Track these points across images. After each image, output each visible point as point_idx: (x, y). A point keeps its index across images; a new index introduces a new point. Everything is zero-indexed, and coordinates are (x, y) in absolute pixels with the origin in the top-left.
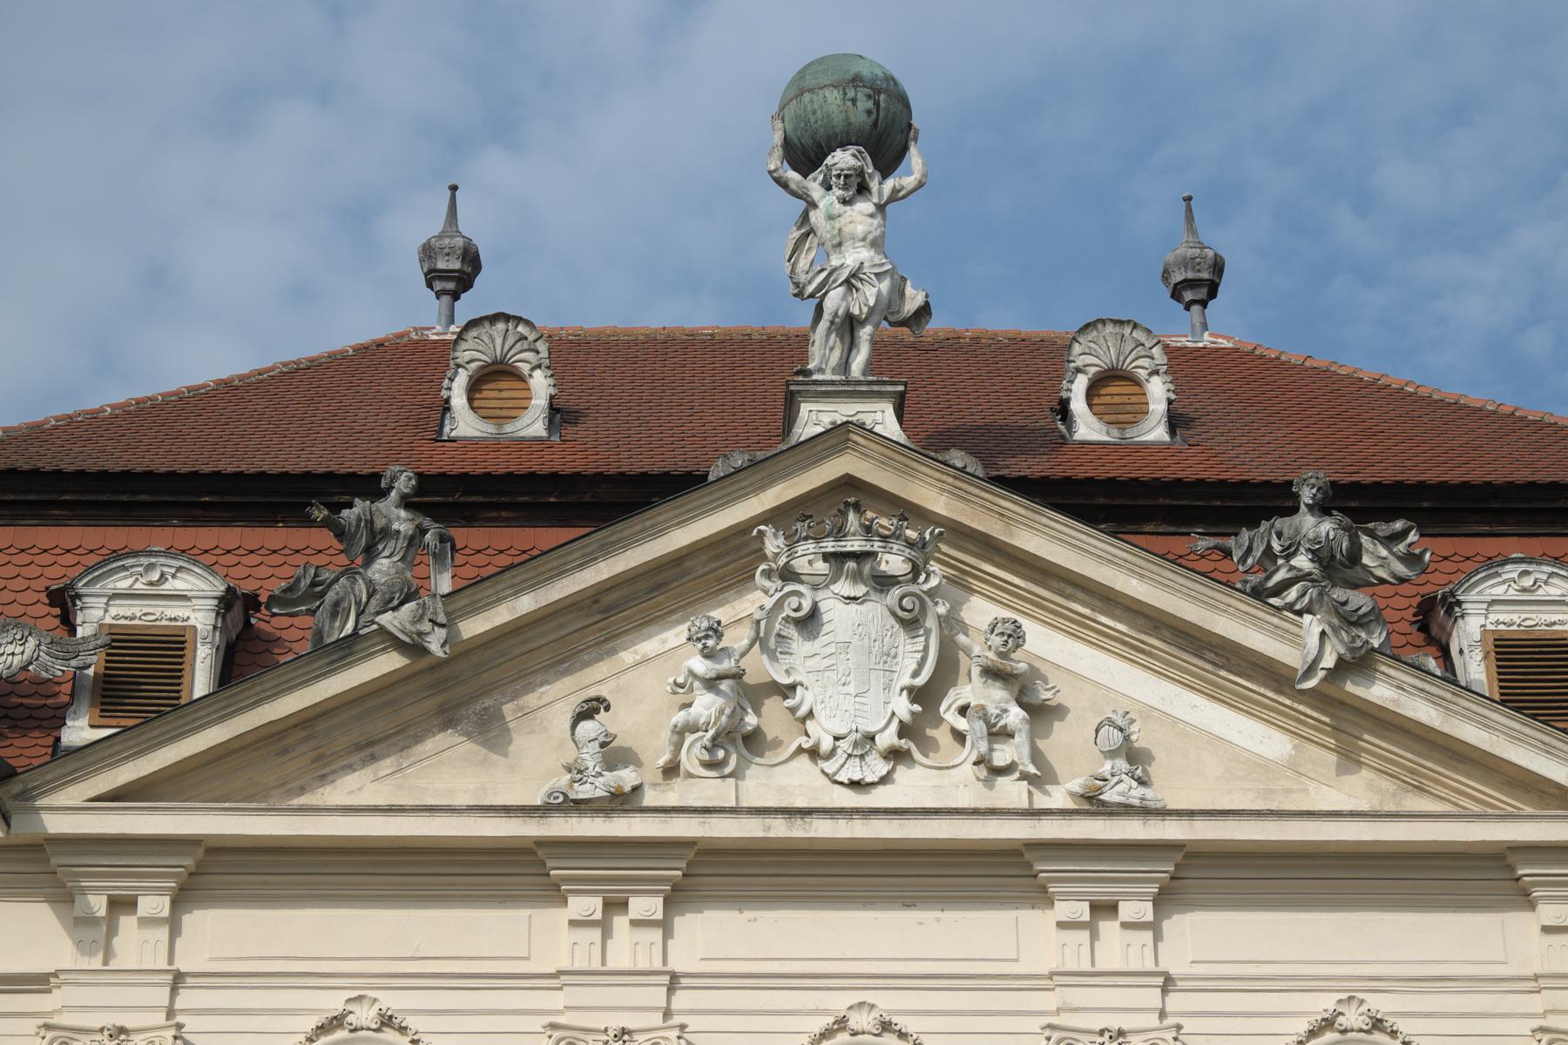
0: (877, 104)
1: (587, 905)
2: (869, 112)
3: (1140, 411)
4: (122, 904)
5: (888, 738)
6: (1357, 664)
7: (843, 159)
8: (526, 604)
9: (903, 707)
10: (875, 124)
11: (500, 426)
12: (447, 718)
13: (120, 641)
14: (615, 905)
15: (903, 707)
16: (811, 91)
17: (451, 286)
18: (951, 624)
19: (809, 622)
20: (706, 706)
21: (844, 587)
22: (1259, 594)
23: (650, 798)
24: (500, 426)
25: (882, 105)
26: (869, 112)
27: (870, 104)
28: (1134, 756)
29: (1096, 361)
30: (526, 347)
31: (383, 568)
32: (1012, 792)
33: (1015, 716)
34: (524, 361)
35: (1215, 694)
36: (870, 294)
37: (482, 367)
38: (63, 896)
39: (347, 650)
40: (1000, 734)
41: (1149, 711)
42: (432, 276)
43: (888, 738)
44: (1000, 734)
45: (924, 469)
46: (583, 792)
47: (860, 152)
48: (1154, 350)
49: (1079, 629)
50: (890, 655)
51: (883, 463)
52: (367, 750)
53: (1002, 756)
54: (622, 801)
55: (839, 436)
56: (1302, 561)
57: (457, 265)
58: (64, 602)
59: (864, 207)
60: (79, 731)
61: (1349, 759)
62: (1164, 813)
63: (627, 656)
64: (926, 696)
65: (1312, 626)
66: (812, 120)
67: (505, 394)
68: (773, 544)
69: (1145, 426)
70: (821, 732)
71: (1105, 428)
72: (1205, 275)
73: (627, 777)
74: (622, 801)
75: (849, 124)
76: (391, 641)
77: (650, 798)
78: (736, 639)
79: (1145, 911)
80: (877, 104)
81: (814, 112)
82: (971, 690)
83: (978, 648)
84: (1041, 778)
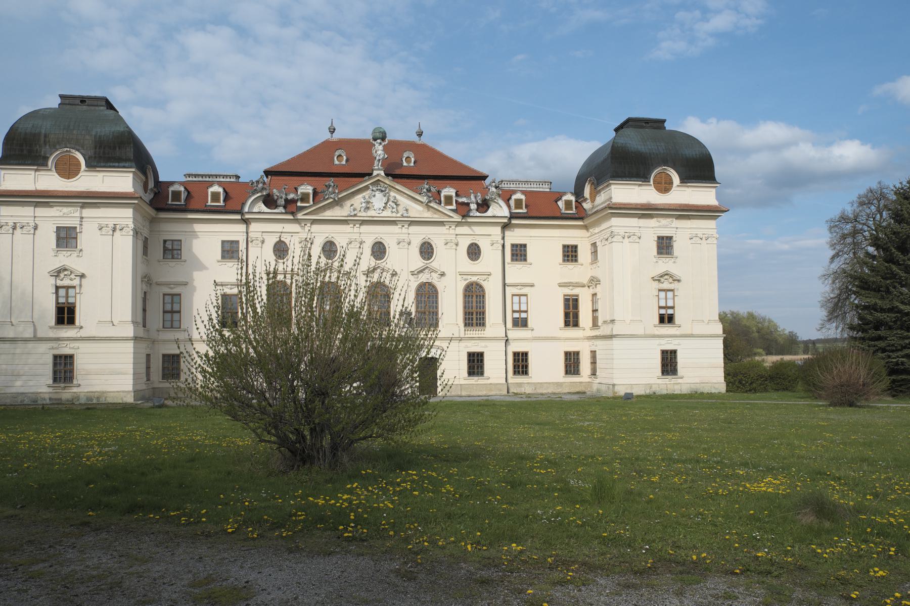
1: (352, 225)
3: (411, 162)
4: (305, 225)
5: (382, 208)
6: (430, 202)
7: (379, 141)
8: (345, 194)
9: (384, 205)
12: (337, 205)
13: (302, 193)
14: (355, 225)
15: (384, 205)
18: (389, 196)
19: (374, 196)
20: (364, 205)
21: (378, 192)
22: (420, 194)
23: (358, 215)
28: (407, 210)
31: (330, 189)
32: (394, 215)
33: (395, 206)
34: (343, 155)
35: (416, 203)
36: (381, 157)
38: (300, 224)
39: (328, 199)
40: (393, 208)
41: (408, 205)
42: (330, 131)
43: (382, 208)
44: (393, 208)
46: (352, 214)
49: (402, 196)
50: (382, 199)
52: (329, 208)
53: (394, 210)
54: (355, 215)
55: (378, 175)
56: (425, 190)
58: (296, 189)
59: (381, 146)
60: (299, 204)
61: (429, 210)
62: (409, 217)
63: (356, 198)
64: (386, 204)
65: (425, 198)
68: (371, 187)
70: (375, 208)
73: (356, 212)
74: (355, 215)
76: (331, 198)
77: (358, 215)
78: (367, 197)
79: (407, 227)
82: (390, 203)
83: (392, 199)
84: (398, 212)
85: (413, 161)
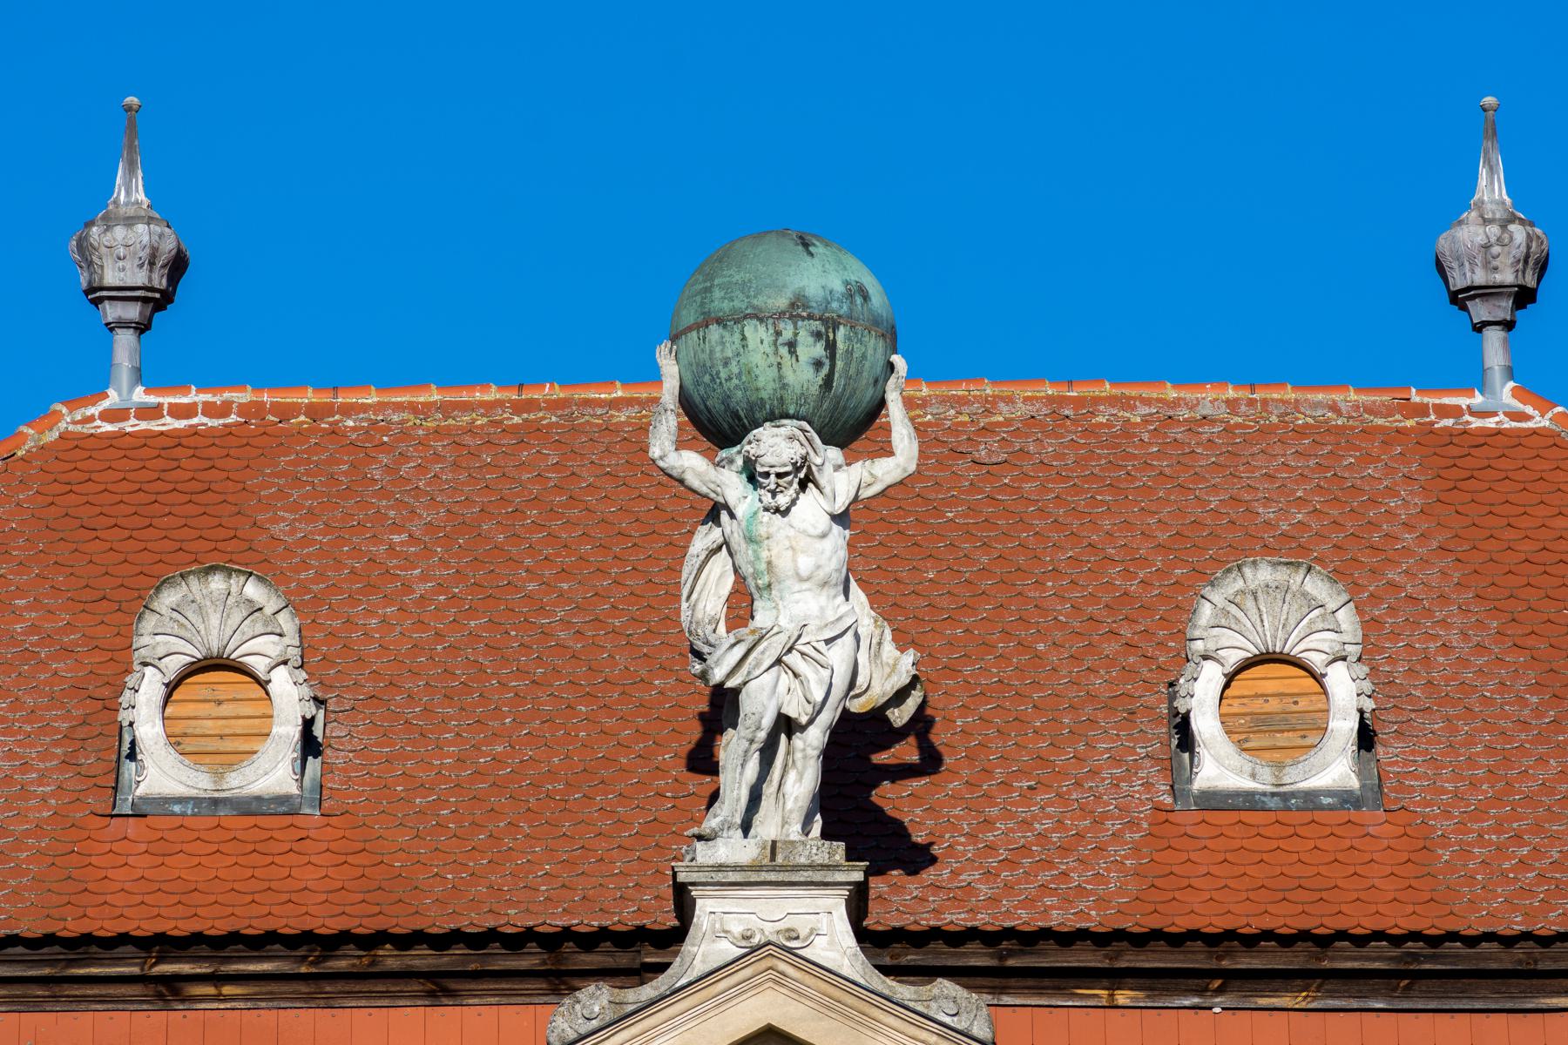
0: (831, 347)
2: (818, 364)
10: (828, 382)
11: (218, 776)
16: (720, 321)
17: (133, 312)
24: (218, 776)
25: (841, 346)
26: (818, 364)
27: (819, 350)
29: (1241, 641)
30: (259, 629)
37: (193, 663)
45: (891, 1020)
47: (804, 431)
48: (1341, 615)
51: (829, 1008)
57: (139, 278)
66: (723, 375)
67: (226, 709)
69: (1315, 758)
71: (1248, 767)
72: (1507, 277)
75: (784, 386)
80: (831, 347)
81: (726, 363)
85: (1344, 726)
